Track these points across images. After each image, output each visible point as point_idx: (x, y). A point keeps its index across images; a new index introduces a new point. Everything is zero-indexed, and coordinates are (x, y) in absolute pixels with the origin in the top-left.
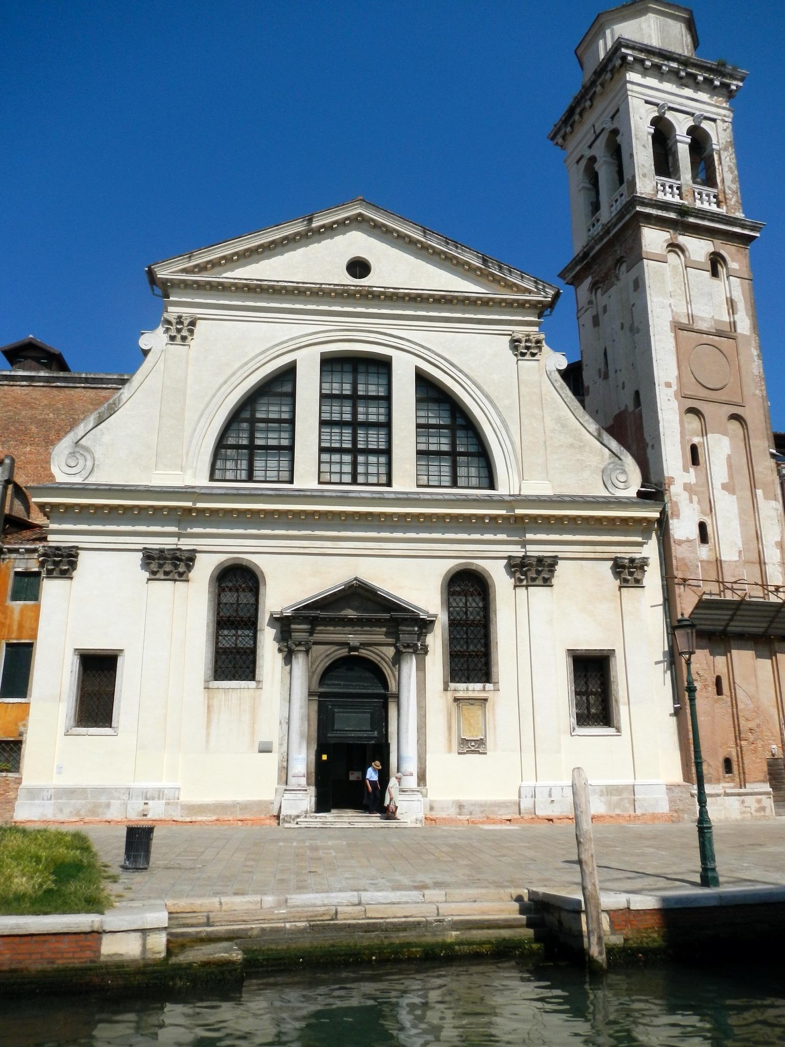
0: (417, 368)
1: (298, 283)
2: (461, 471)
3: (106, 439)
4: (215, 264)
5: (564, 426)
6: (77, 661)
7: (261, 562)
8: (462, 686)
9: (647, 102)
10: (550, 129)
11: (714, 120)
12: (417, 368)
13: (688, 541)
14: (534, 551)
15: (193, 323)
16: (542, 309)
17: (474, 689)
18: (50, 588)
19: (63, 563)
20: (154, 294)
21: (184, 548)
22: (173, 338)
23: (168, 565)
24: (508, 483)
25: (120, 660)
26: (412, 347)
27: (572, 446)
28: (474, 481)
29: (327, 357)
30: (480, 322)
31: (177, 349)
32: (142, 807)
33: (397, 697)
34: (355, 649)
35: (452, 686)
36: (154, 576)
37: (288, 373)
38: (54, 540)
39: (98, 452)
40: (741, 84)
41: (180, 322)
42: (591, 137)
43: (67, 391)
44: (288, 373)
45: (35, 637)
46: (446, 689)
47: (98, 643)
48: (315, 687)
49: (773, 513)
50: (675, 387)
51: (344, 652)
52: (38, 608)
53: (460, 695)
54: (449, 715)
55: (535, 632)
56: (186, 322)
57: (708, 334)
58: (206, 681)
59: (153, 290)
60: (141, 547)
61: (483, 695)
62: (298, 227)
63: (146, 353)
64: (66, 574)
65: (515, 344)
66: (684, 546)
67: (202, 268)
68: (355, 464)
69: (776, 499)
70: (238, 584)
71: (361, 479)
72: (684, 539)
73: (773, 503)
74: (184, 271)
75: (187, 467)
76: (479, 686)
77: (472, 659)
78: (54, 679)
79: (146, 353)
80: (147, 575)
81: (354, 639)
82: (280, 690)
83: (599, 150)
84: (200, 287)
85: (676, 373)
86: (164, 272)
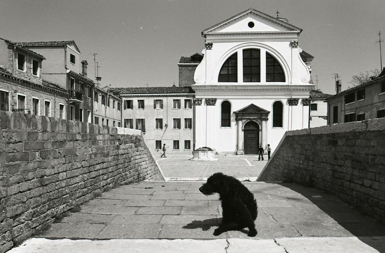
0: (266, 51)
7: (231, 101)
12: (266, 51)
14: (294, 97)
16: (298, 34)
23: (211, 102)
26: (266, 46)
33: (261, 130)
34: (252, 120)
37: (236, 54)
48: (243, 128)
51: (249, 121)
59: (202, 35)
60: (205, 98)
65: (291, 44)
70: (226, 106)
75: (214, 81)
81: (252, 118)
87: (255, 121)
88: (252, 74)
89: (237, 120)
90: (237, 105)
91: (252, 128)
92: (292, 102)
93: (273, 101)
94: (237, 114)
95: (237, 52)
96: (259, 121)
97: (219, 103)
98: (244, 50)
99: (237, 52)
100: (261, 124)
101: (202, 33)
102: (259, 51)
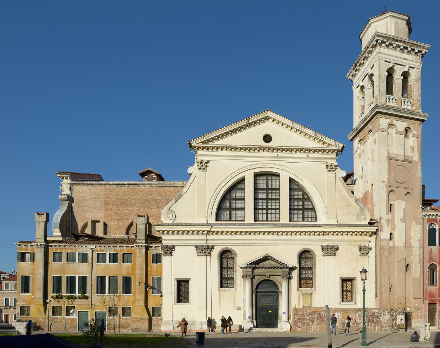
2: (306, 216)
4: (213, 139)
5: (343, 198)
9: (385, 61)
11: (414, 68)
13: (385, 240)
14: (330, 244)
15: (207, 162)
17: (308, 290)
18: (166, 259)
19: (170, 250)
24: (322, 219)
25: (190, 282)
27: (346, 206)
29: (257, 174)
31: (202, 173)
32: (200, 326)
36: (199, 254)
39: (177, 212)
40: (427, 51)
41: (201, 163)
43: (164, 188)
45: (162, 275)
46: (298, 290)
49: (419, 229)
50: (386, 183)
52: (162, 265)
53: (303, 292)
54: (299, 298)
56: (204, 163)
57: (401, 161)
60: (194, 244)
62: (244, 122)
63: (190, 175)
66: (384, 241)
67: (208, 141)
68: (267, 214)
69: (420, 224)
71: (269, 219)
72: (384, 239)
73: (419, 226)
74: (203, 142)
76: (309, 289)
77: (306, 281)
79: (190, 175)
80: (197, 254)
82: (242, 291)
85: (387, 177)
86: (194, 143)
87: (270, 278)
90: (245, 256)
101: (190, 144)
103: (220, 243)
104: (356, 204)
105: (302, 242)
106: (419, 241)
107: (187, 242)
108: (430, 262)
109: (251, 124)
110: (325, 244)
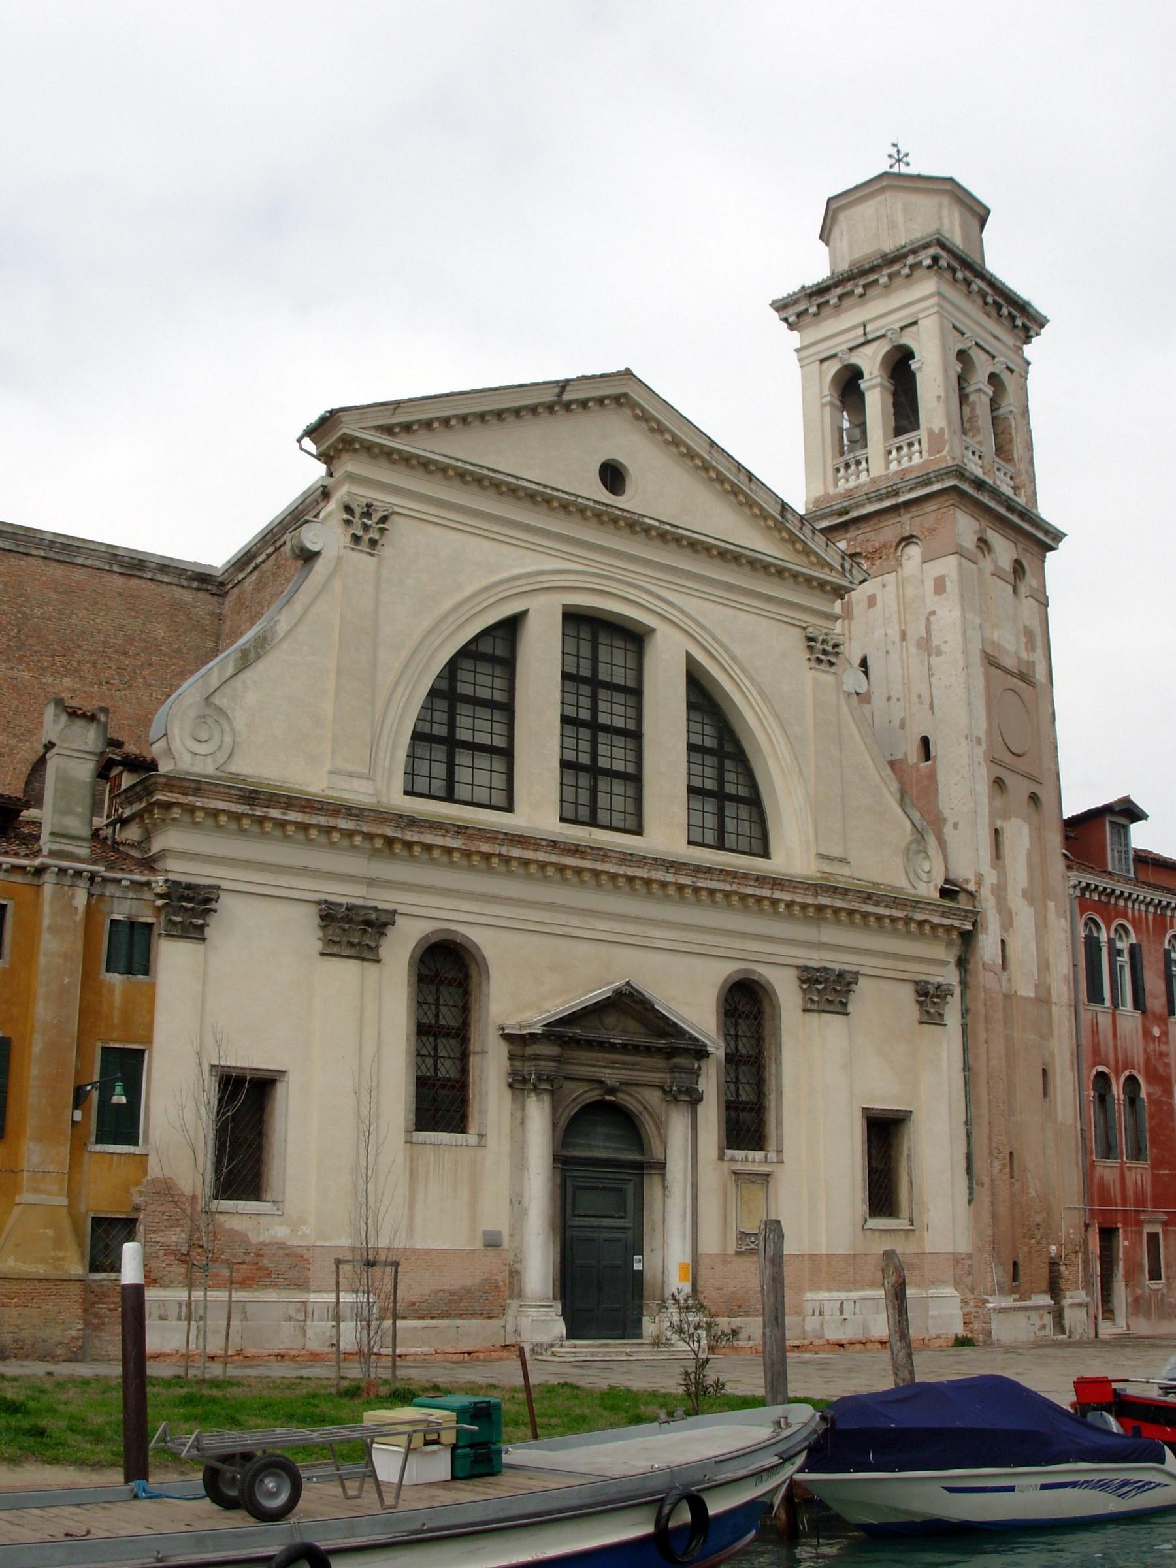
1: (545, 487)
3: (251, 698)
6: (212, 1085)
7: (484, 941)
8: (739, 1154)
10: (781, 293)
18: (173, 958)
19: (191, 909)
20: (302, 449)
21: (381, 906)
22: (356, 539)
23: (352, 931)
25: (280, 1088)
28: (744, 844)
30: (769, 599)
31: (361, 560)
34: (612, 1091)
35: (729, 1153)
37: (511, 627)
38: (179, 870)
39: (240, 719)
41: (367, 514)
42: (857, 336)
44: (511, 627)
45: (149, 1040)
46: (721, 1158)
47: (248, 1056)
51: (594, 1095)
52: (153, 986)
53: (738, 1167)
54: (725, 1195)
55: (824, 1076)
56: (376, 517)
58: (408, 1132)
61: (765, 1169)
64: (195, 932)
78: (177, 1115)
80: (319, 946)
81: (611, 1076)
82: (512, 1153)
83: (871, 362)
84: (388, 454)
87: (623, 1098)
88: (601, 775)
89: (518, 1084)
91: (601, 1146)
92: (829, 990)
93: (719, 973)
94: (517, 1041)
95: (524, 613)
96: (654, 1097)
97: (399, 949)
98: (573, 618)
99: (524, 613)
100: (661, 1125)
102: (634, 638)
103: (425, 901)
104: (899, 810)
105: (737, 944)
106: (1066, 977)
107: (283, 880)
108: (1095, 1064)
109: (567, 406)
110: (814, 959)
